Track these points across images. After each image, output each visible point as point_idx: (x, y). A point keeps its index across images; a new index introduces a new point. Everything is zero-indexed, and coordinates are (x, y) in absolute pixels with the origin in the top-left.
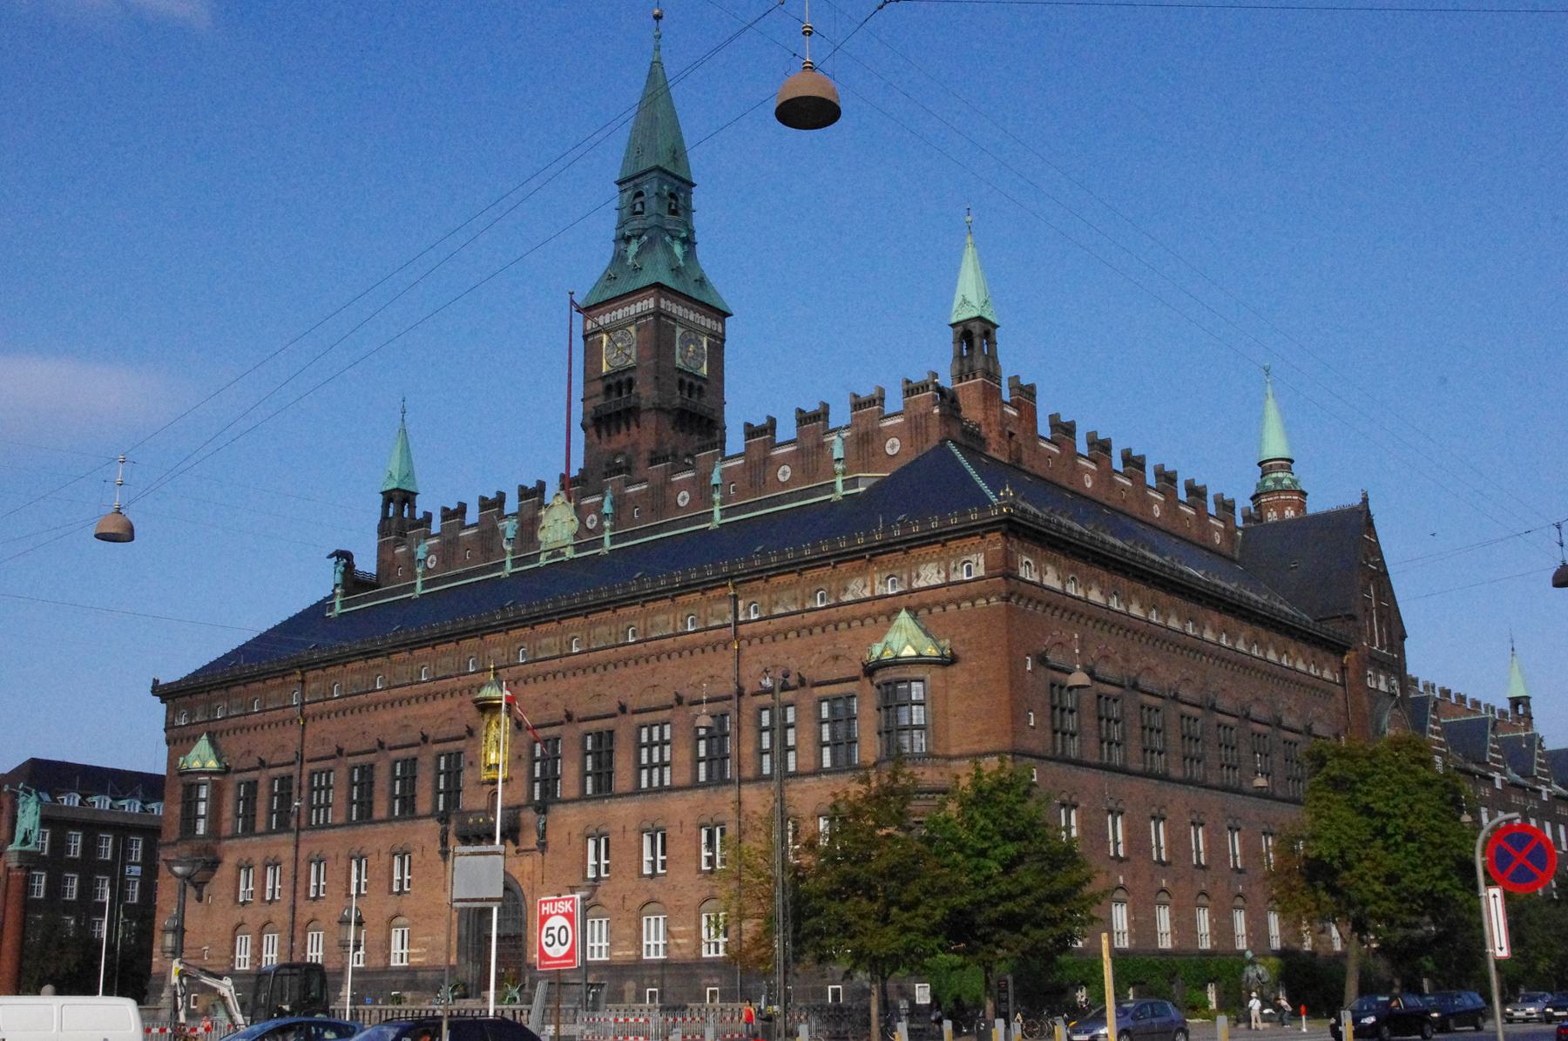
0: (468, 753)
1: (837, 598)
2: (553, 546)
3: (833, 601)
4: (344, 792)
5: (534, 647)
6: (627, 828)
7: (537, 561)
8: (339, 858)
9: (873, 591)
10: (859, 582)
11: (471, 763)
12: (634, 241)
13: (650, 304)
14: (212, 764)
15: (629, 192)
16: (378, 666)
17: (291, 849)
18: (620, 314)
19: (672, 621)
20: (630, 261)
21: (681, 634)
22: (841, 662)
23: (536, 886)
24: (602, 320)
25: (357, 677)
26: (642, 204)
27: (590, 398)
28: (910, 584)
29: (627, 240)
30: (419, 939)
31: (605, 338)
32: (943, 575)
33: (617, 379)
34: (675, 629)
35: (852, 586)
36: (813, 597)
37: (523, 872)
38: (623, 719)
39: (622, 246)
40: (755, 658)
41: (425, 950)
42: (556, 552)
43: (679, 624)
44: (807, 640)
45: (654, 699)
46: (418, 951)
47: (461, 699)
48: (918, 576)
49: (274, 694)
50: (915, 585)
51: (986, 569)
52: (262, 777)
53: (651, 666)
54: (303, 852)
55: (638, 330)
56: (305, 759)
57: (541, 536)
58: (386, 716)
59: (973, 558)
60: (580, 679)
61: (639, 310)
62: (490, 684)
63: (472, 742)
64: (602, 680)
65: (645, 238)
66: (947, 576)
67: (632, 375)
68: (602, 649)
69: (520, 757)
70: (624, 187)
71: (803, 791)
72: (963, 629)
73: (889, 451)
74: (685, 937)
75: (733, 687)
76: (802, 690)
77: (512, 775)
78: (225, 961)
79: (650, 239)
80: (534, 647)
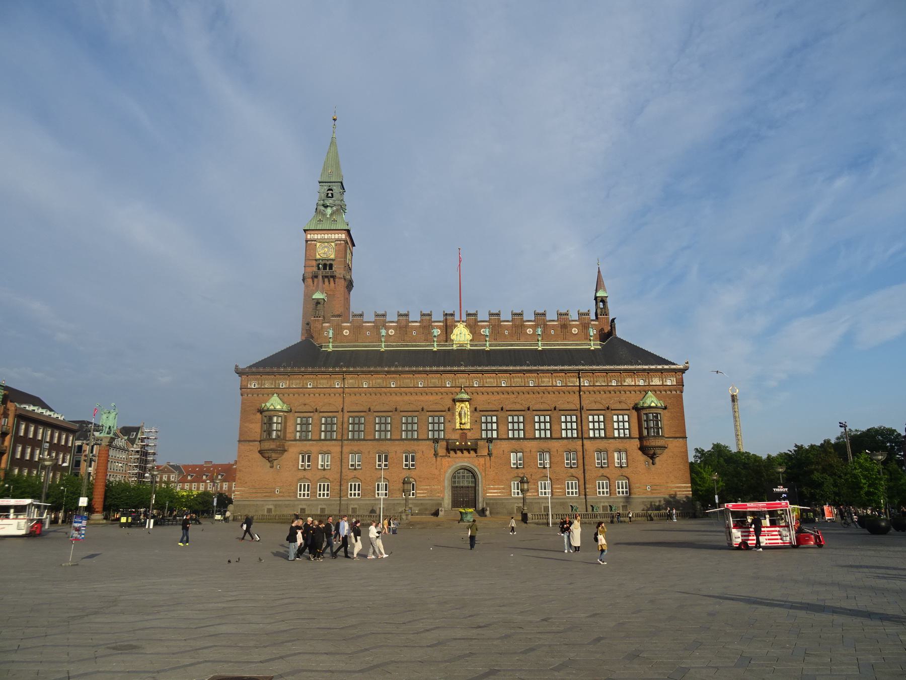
0: (448, 418)
1: (621, 384)
2: (461, 342)
3: (620, 384)
4: (373, 427)
5: (483, 381)
6: (532, 451)
7: (453, 347)
8: (371, 452)
9: (635, 383)
10: (630, 379)
11: (449, 421)
12: (329, 208)
13: (343, 236)
14: (285, 408)
15: (326, 188)
16: (393, 378)
17: (341, 447)
18: (326, 236)
19: (551, 381)
20: (328, 216)
21: (555, 386)
22: (622, 404)
23: (487, 469)
24: (316, 237)
25: (379, 381)
26: (332, 194)
27: (308, 266)
28: (649, 383)
29: (326, 207)
30: (422, 487)
31: (318, 244)
32: (661, 382)
33: (324, 262)
34: (552, 384)
35: (627, 381)
36: (611, 381)
37: (479, 464)
38: (529, 412)
39: (323, 208)
40: (587, 398)
41: (426, 491)
42: (461, 345)
43: (554, 383)
44: (608, 395)
45: (542, 407)
46: (422, 492)
47: (441, 396)
48: (652, 381)
49: (325, 381)
50: (651, 384)
51: (676, 383)
52: (316, 415)
53: (540, 395)
54: (346, 449)
55: (336, 245)
56: (345, 411)
57: (453, 337)
58: (398, 398)
59: (672, 379)
60: (506, 396)
61: (337, 237)
62: (462, 393)
63: (449, 413)
64: (517, 397)
65: (334, 208)
66: (663, 383)
67: (331, 262)
68: (518, 386)
69: (476, 421)
70: (322, 184)
71: (609, 443)
72: (668, 399)
73: (573, 332)
74: (560, 489)
75: (578, 406)
76: (607, 411)
77: (474, 427)
78: (292, 494)
79: (337, 210)
80: (483, 381)
